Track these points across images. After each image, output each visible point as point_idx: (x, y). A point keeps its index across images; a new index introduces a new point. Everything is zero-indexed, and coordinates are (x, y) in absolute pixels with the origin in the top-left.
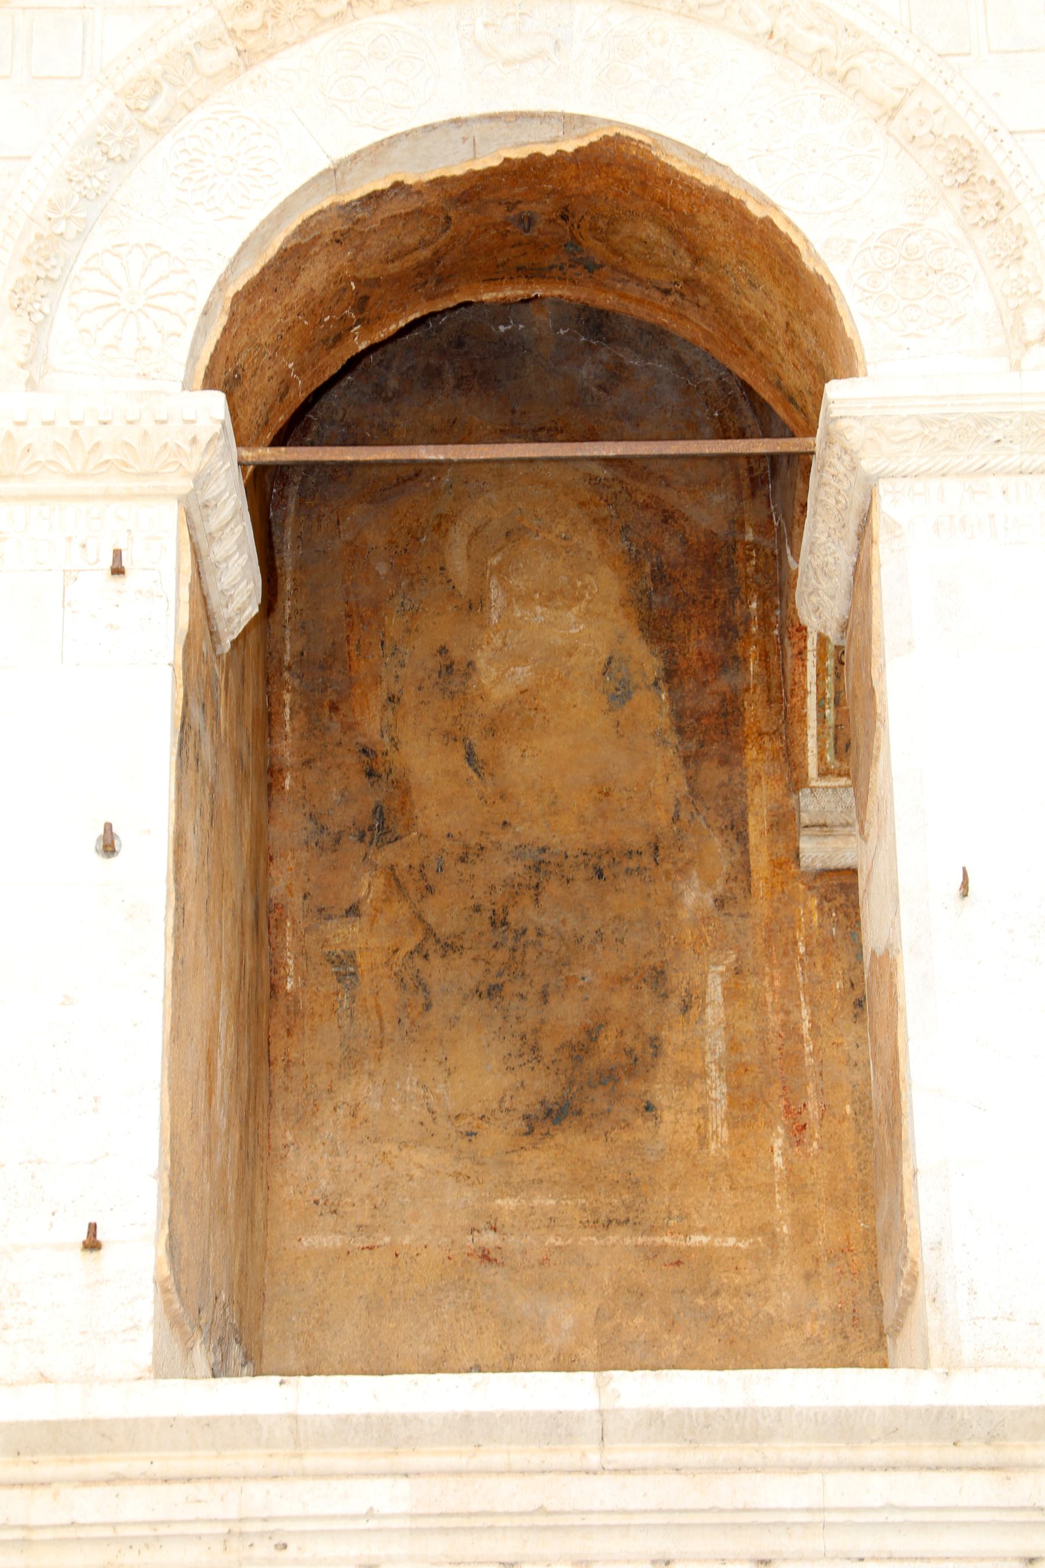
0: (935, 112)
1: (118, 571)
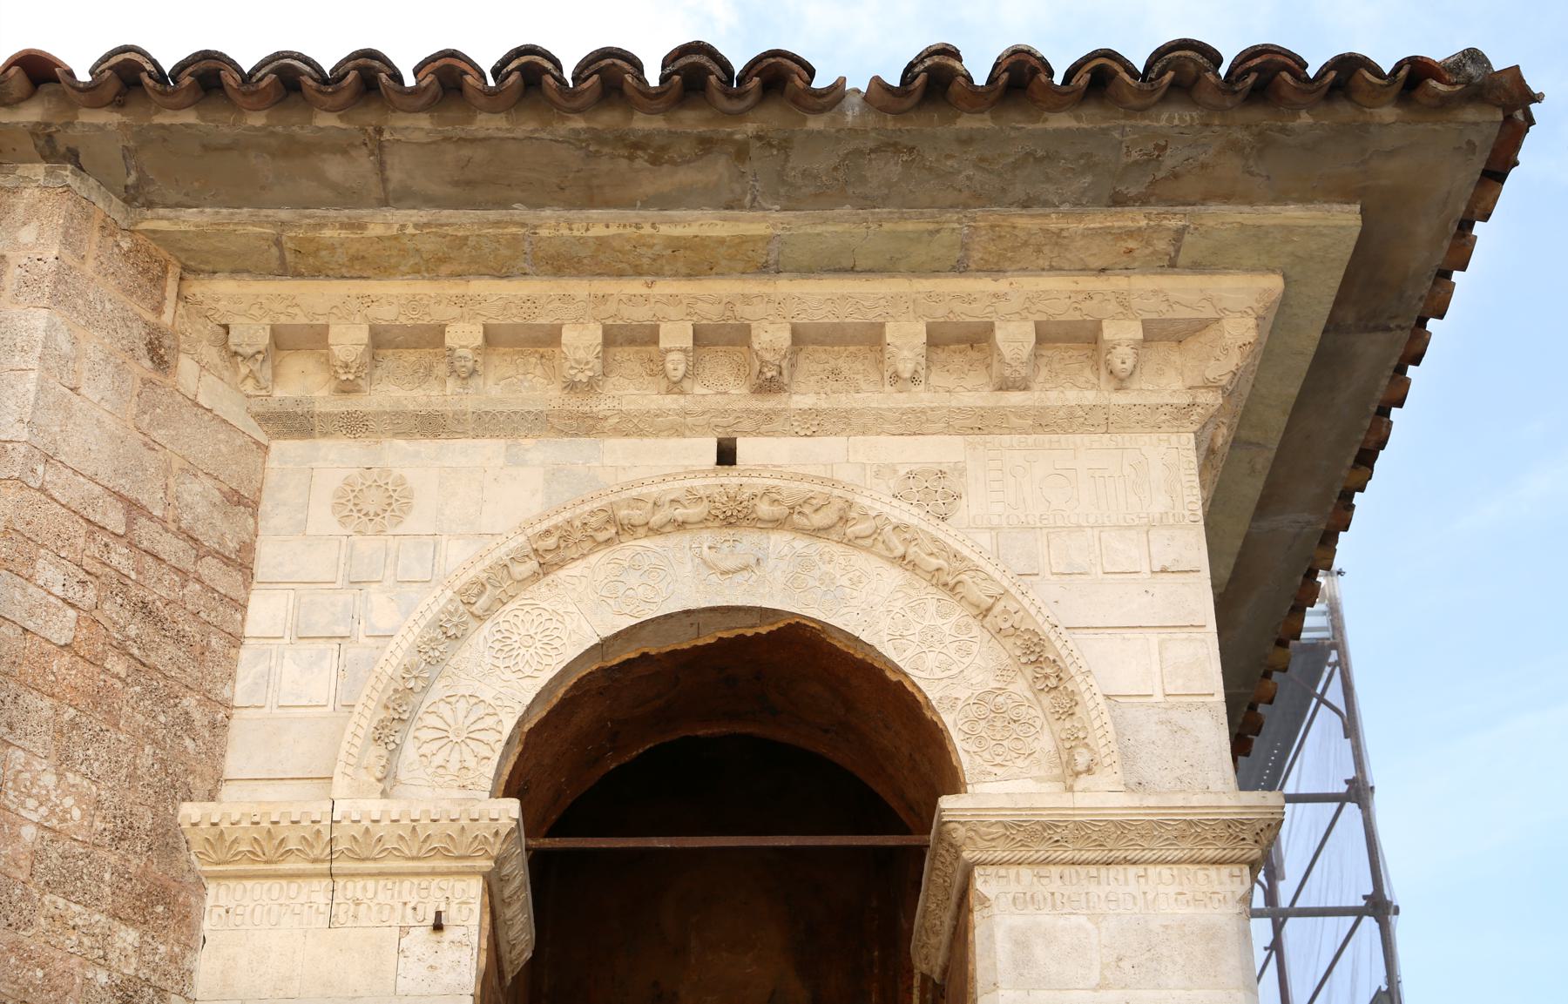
1: (438, 927)
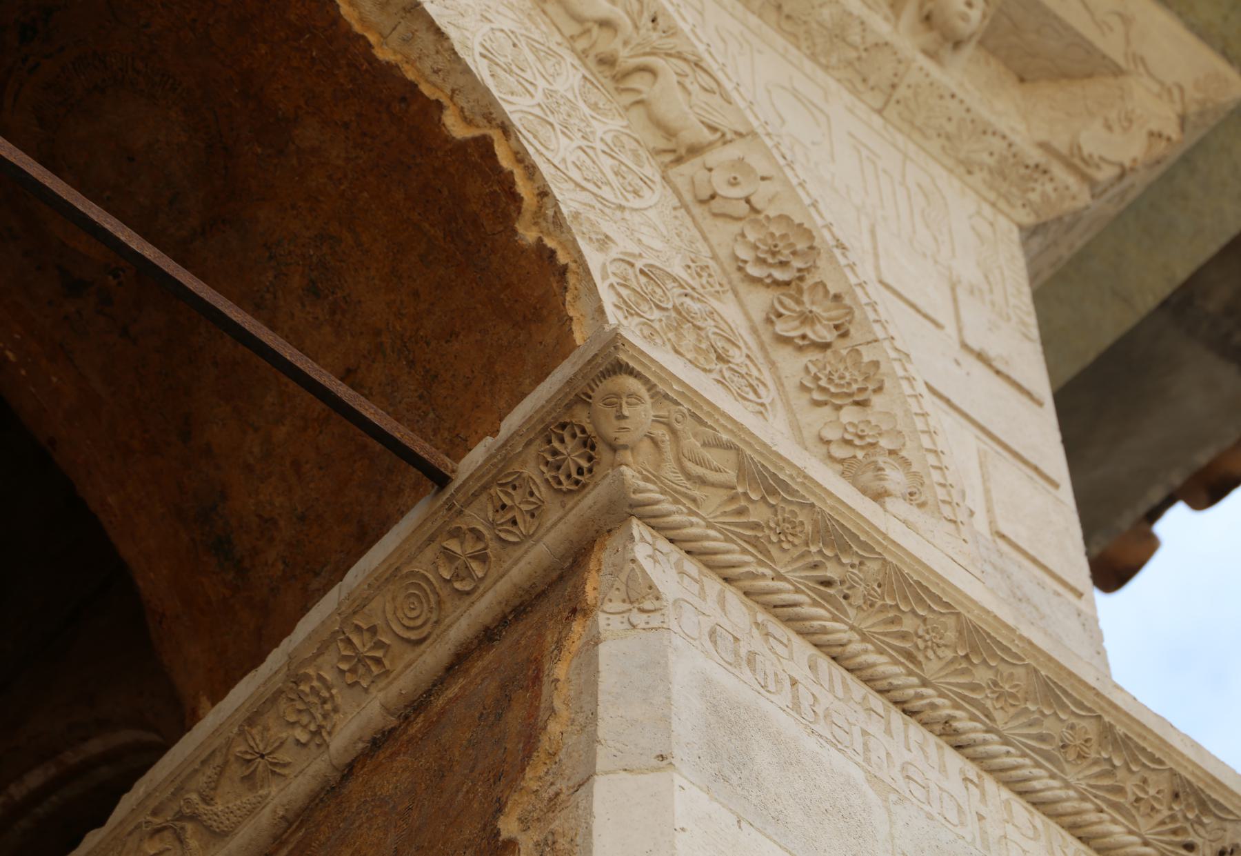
0: (763, 179)
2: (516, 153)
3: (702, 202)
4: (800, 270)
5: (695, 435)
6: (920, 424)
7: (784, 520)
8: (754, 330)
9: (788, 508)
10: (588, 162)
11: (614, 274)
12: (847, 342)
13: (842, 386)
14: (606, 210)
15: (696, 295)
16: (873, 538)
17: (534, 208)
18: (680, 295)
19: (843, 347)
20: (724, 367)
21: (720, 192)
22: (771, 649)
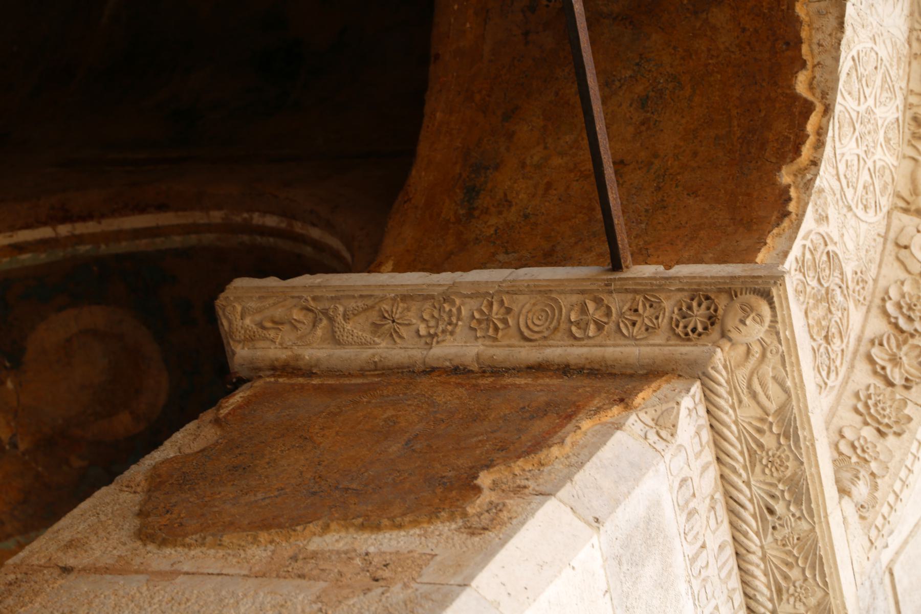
2: (820, 128)
3: (897, 245)
4: (916, 330)
5: (774, 368)
6: (903, 473)
7: (779, 457)
8: (859, 340)
9: (787, 452)
10: (855, 168)
11: (812, 241)
12: (905, 393)
13: (880, 414)
14: (840, 203)
15: (845, 292)
16: (819, 511)
17: (802, 166)
18: (837, 284)
19: (900, 394)
20: (824, 345)
21: (913, 248)
22: (708, 518)
